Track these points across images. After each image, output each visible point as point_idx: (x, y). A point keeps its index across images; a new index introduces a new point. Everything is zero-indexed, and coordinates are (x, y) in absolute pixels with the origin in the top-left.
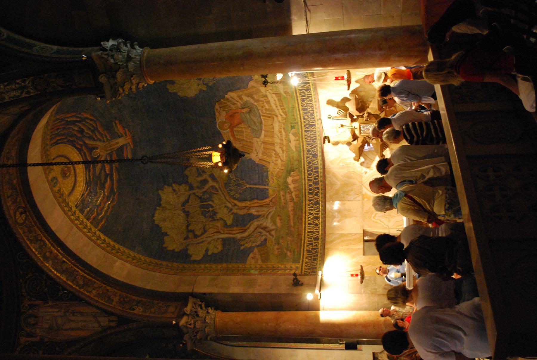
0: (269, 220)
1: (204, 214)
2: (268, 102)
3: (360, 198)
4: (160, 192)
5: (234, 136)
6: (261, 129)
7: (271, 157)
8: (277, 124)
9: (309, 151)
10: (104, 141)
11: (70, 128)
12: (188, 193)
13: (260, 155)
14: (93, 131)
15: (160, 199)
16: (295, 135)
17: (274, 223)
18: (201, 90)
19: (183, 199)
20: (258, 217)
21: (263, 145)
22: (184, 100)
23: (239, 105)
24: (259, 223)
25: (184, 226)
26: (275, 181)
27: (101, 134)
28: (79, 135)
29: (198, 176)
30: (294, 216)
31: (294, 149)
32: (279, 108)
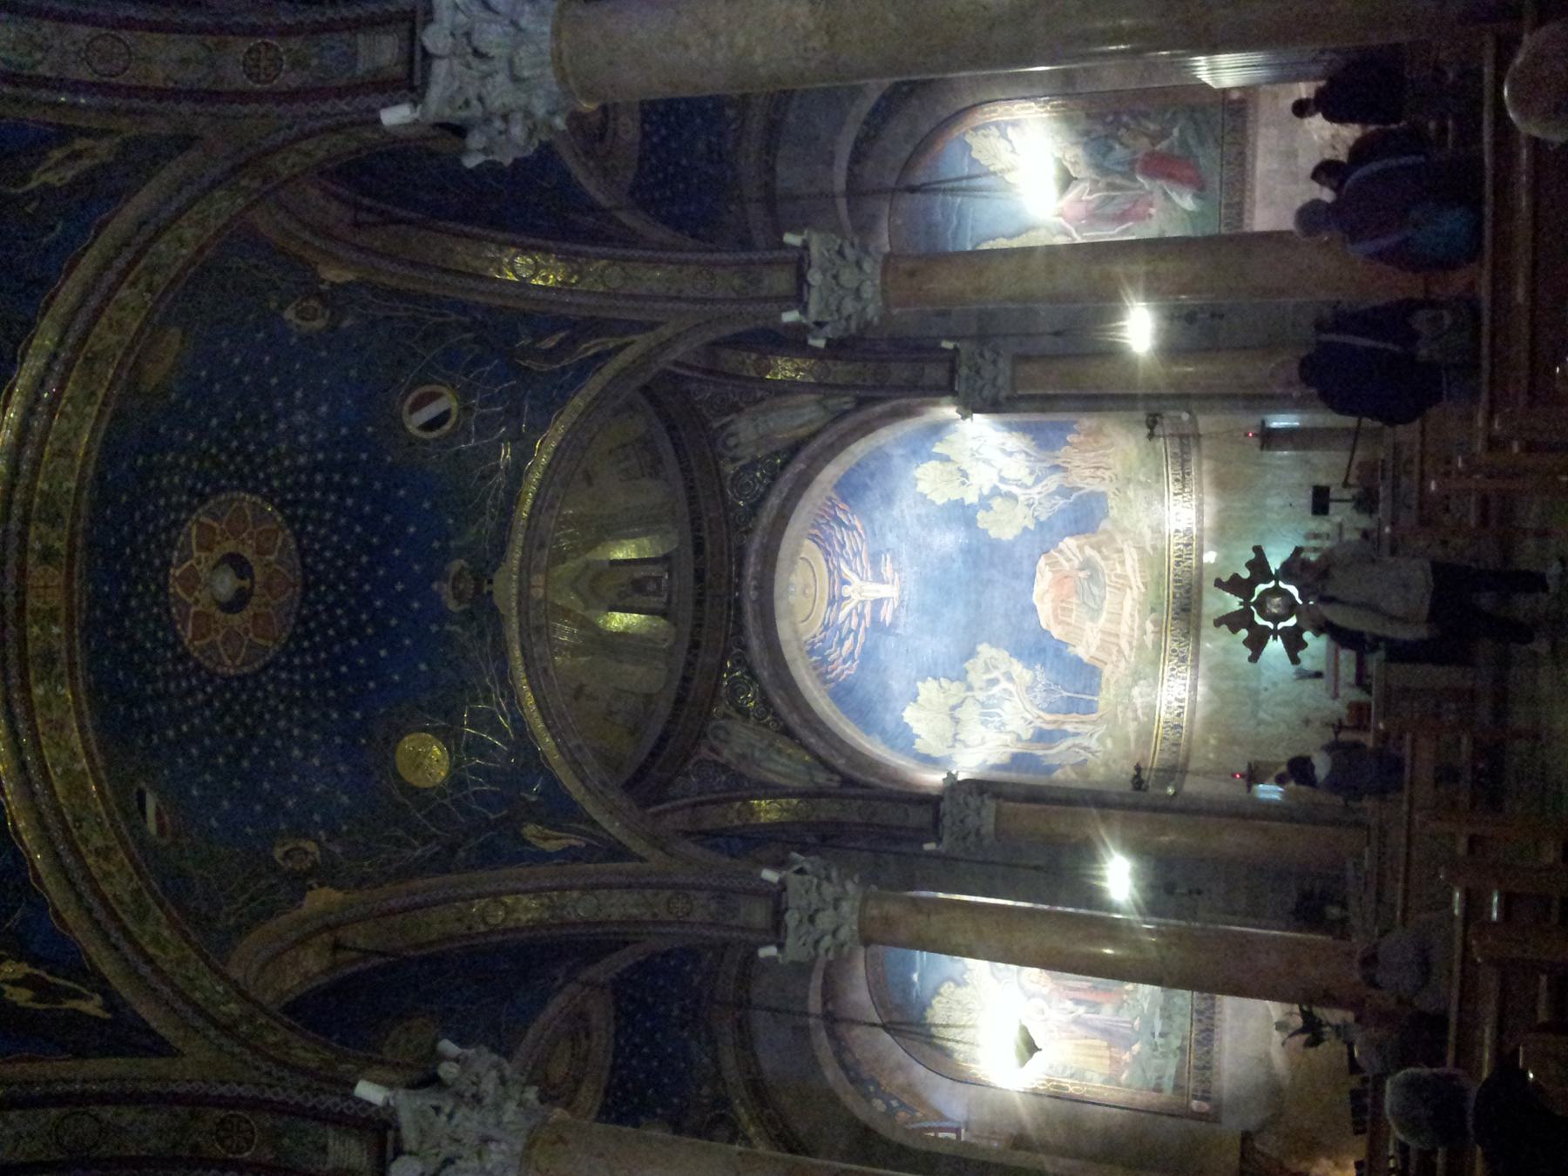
0: (1094, 740)
1: (984, 723)
2: (1122, 563)
3: (1252, 722)
4: (919, 684)
5: (1056, 617)
6: (1101, 609)
7: (1110, 655)
8: (1130, 602)
9: (1174, 651)
10: (861, 579)
11: (832, 528)
12: (963, 695)
13: (1093, 651)
14: (855, 555)
15: (917, 694)
16: (1156, 623)
17: (1104, 744)
18: (1025, 529)
19: (953, 701)
20: (1076, 735)
21: (1100, 635)
22: (995, 545)
23: (1076, 563)
24: (1078, 740)
25: (949, 735)
26: (1112, 691)
27: (863, 567)
28: (837, 549)
29: (984, 673)
30: (1137, 740)
31: (1150, 646)
32: (1138, 575)
